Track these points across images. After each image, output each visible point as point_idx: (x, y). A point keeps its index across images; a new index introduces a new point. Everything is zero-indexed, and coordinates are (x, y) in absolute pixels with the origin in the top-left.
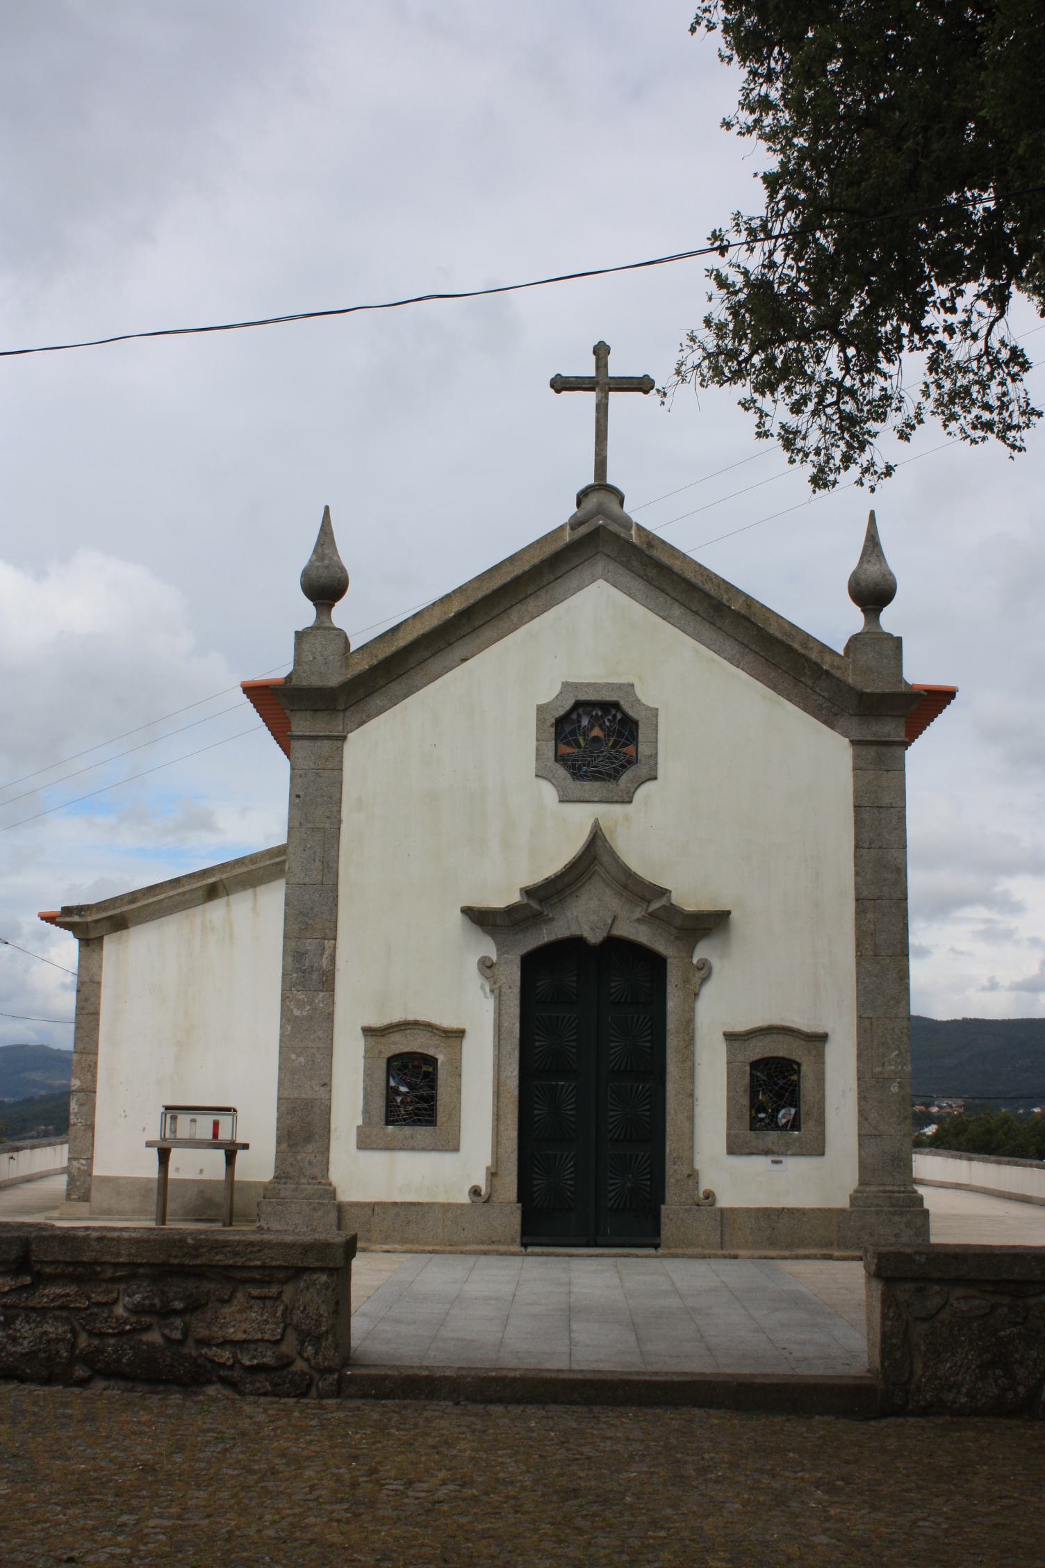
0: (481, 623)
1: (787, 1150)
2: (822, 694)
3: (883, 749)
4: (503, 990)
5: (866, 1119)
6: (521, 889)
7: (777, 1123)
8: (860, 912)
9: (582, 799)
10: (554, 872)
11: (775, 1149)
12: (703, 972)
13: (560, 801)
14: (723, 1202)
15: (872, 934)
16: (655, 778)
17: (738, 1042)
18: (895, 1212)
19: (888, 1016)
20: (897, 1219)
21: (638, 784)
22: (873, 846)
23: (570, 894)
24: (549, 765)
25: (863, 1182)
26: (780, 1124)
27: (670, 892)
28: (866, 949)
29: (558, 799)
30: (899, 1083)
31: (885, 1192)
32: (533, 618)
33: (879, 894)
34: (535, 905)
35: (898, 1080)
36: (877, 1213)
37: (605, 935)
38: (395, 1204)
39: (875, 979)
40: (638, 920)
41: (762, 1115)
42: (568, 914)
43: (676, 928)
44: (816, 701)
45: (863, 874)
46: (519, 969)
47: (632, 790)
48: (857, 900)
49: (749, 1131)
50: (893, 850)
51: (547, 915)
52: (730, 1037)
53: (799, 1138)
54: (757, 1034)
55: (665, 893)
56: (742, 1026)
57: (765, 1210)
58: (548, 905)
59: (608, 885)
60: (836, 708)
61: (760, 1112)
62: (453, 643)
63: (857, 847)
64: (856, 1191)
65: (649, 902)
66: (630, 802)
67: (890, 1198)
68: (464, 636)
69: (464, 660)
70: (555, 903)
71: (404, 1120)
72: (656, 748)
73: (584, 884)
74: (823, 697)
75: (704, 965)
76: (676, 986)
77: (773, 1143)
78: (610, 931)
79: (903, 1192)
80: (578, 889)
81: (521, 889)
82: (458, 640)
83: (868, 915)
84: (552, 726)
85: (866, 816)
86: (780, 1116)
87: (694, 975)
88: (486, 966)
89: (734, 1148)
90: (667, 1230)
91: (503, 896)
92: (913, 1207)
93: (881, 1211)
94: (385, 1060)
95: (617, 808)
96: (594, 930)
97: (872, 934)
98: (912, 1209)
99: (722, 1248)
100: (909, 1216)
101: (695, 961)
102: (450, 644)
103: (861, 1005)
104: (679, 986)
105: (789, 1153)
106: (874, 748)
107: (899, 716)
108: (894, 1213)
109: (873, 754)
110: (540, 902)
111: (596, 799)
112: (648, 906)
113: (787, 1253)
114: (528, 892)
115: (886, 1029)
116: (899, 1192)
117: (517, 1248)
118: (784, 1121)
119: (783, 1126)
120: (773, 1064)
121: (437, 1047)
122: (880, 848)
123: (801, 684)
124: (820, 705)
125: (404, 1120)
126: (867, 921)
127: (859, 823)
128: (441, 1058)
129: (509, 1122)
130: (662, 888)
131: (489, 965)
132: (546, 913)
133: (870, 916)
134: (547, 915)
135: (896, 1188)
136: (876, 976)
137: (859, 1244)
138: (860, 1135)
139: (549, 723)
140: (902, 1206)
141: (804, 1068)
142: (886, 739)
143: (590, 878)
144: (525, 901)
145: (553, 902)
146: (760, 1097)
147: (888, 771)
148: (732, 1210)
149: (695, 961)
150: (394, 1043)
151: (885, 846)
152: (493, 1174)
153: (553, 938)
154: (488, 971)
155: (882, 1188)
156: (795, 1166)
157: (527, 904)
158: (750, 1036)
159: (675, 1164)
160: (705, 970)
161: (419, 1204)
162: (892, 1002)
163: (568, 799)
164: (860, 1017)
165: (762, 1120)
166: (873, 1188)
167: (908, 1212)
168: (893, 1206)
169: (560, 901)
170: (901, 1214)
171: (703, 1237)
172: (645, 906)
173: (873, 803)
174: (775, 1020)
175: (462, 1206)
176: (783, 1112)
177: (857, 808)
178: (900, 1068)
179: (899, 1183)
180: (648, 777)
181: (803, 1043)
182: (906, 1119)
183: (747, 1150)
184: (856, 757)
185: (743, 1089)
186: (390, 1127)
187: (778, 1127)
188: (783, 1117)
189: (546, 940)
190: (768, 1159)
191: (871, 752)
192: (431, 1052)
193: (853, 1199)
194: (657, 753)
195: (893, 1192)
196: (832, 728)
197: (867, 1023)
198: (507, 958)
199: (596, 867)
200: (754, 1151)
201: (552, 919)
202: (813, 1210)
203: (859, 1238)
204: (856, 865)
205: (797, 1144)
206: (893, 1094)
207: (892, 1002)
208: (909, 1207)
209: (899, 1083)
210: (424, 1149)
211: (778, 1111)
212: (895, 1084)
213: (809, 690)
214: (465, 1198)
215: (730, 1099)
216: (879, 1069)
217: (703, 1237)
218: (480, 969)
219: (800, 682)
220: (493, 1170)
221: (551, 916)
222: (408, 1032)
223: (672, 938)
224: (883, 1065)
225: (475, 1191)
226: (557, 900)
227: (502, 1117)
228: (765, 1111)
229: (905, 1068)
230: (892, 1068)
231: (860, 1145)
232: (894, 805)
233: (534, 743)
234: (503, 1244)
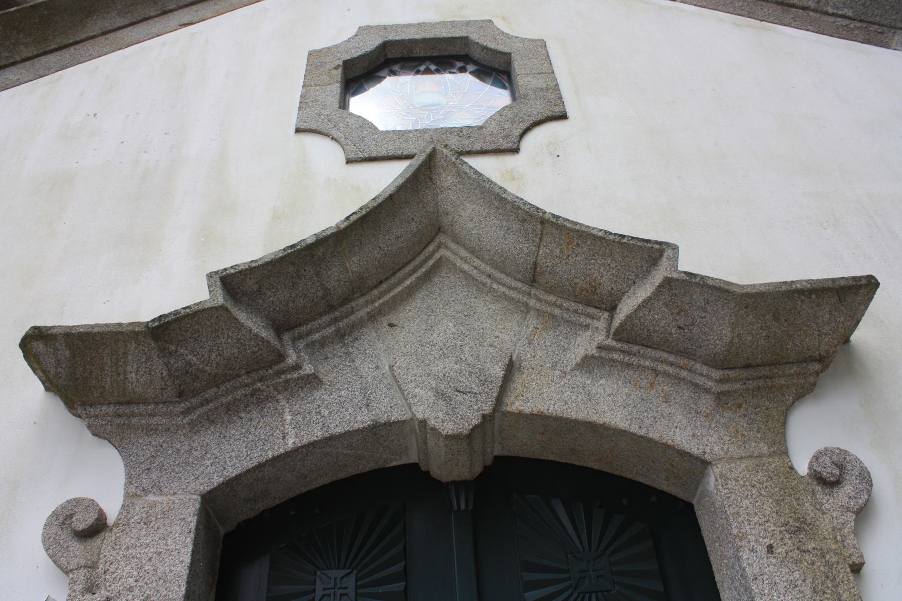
2: (840, 12)
6: (210, 276)
9: (399, 153)
12: (847, 488)
13: (349, 161)
16: (563, 117)
23: (372, 318)
27: (675, 248)
29: (343, 159)
37: (487, 408)
40: (587, 364)
42: (366, 369)
43: (715, 363)
46: (189, 540)
47: (517, 133)
51: (297, 367)
55: (661, 253)
58: (301, 344)
59: (482, 288)
62: (171, 11)
65: (612, 309)
66: (515, 150)
70: (323, 343)
72: (555, 79)
73: (410, 292)
74: (842, 16)
75: (841, 467)
76: (770, 549)
78: (499, 400)
80: (394, 304)
81: (210, 276)
87: (818, 506)
96: (447, 399)
101: (802, 467)
102: (165, 13)
104: (780, 550)
110: (279, 329)
112: (612, 317)
130: (648, 241)
131: (81, 526)
132: (292, 358)
134: (297, 367)
143: (427, 277)
144: (220, 300)
149: (802, 467)
154: (77, 547)
157: (222, 308)
163: (366, 155)
169: (341, 336)
172: (601, 324)
180: (548, 113)
189: (291, 443)
194: (557, 85)
198: (153, 505)
199: (443, 252)
201: (313, 381)
213: (811, 14)
218: (51, 544)
221: (308, 369)
223: (706, 403)
226: (330, 330)
233: (299, 90)
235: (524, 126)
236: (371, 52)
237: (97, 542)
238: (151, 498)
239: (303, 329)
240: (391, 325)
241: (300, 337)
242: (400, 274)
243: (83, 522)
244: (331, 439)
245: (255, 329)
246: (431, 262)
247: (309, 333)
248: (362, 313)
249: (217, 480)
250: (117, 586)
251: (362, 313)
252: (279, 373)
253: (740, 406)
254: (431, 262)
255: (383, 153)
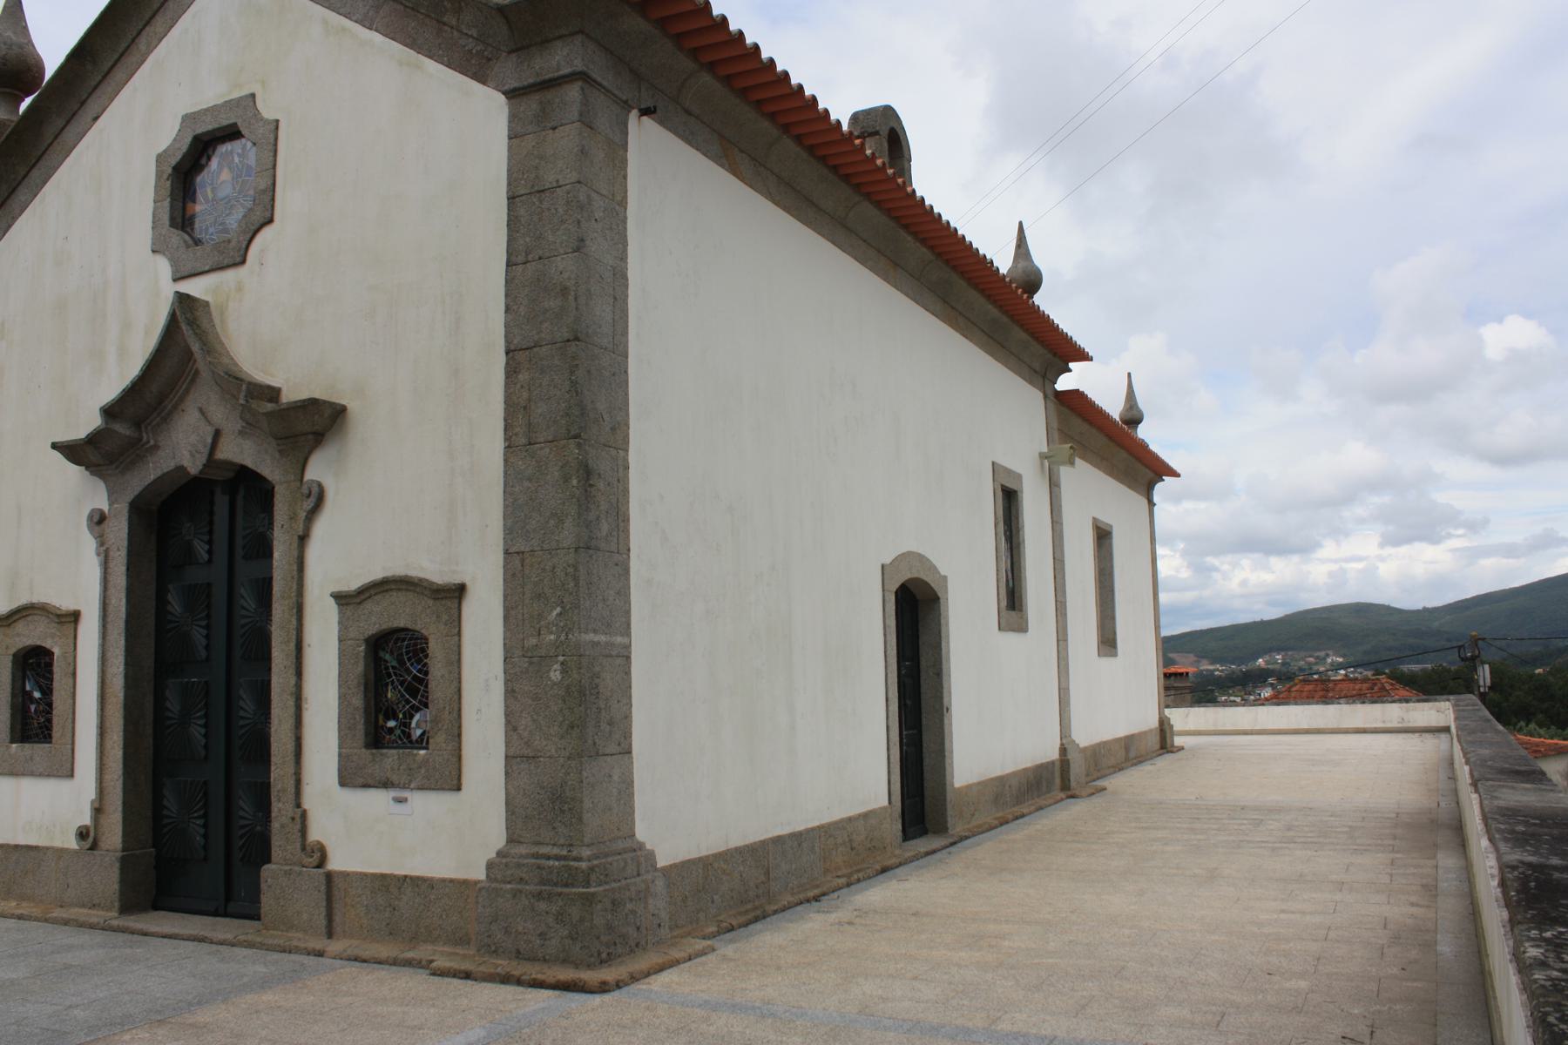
0: (110, 64)
1: (410, 781)
3: (549, 95)
4: (111, 553)
5: (515, 729)
7: (409, 736)
8: (511, 371)
9: (193, 272)
10: (130, 380)
11: (395, 778)
14: (335, 864)
15: (525, 408)
17: (352, 607)
18: (540, 893)
19: (546, 547)
20: (543, 906)
21: (251, 234)
22: (530, 259)
23: (175, 407)
24: (164, 233)
25: (511, 840)
26: (414, 738)
28: (516, 435)
30: (562, 663)
31: (536, 856)
32: (160, 40)
33: (536, 338)
34: (122, 429)
35: (561, 658)
36: (516, 894)
38: (17, 847)
39: (526, 484)
41: (391, 724)
44: (464, 46)
45: (515, 307)
48: (507, 353)
49: (364, 750)
50: (559, 258)
52: (341, 598)
53: (426, 761)
54: (373, 592)
56: (354, 585)
57: (383, 876)
60: (490, 49)
61: (389, 719)
63: (509, 264)
64: (499, 854)
67: (539, 867)
68: (96, 88)
69: (96, 118)
71: (37, 735)
73: (187, 391)
76: (282, 526)
77: (393, 769)
79: (565, 858)
80: (182, 399)
82: (90, 94)
83: (520, 376)
84: (168, 179)
85: (522, 212)
86: (413, 725)
88: (98, 520)
89: (349, 777)
90: (267, 901)
91: (86, 422)
92: (573, 885)
93: (521, 892)
94: (11, 658)
95: (229, 276)
97: (525, 408)
98: (566, 890)
99: (330, 934)
100: (560, 903)
103: (509, 532)
105: (412, 786)
106: (537, 96)
107: (572, 34)
108: (539, 896)
109: (534, 106)
111: (207, 268)
113: (384, 951)
114: (109, 412)
115: (544, 570)
116: (557, 858)
117: (112, 917)
118: (419, 732)
119: (417, 741)
120: (404, 640)
121: (53, 636)
122: (540, 258)
123: (446, 28)
124: (470, 51)
125: (37, 735)
126: (519, 386)
127: (513, 223)
128: (56, 651)
129: (115, 737)
133: (523, 377)
134: (148, 442)
135: (556, 851)
136: (530, 480)
137: (489, 946)
138: (507, 757)
139: (165, 176)
140: (556, 885)
141: (432, 644)
142: (556, 74)
145: (154, 423)
146: (389, 695)
147: (554, 128)
148: (345, 875)
150: (18, 635)
151: (547, 254)
152: (98, 811)
153: (159, 473)
154: (97, 528)
155: (535, 849)
156: (426, 805)
158: (363, 597)
159: (279, 801)
160: (318, 499)
161: (36, 848)
162: (552, 522)
164: (507, 552)
165: (391, 730)
166: (523, 850)
167: (560, 894)
168: (543, 882)
170: (549, 897)
171: (305, 916)
173: (533, 186)
174: (397, 568)
175: (61, 852)
176: (417, 717)
177: (511, 199)
178: (563, 638)
179: (562, 841)
180: (262, 221)
181: (431, 602)
182: (572, 727)
183: (361, 780)
184: (513, 118)
185: (356, 681)
186: (14, 745)
187: (411, 742)
188: (418, 725)
189: (152, 477)
190: (393, 793)
191: (531, 104)
192: (48, 644)
193: (490, 866)
195: (549, 858)
196: (484, 83)
197: (517, 561)
200: (370, 782)
201: (156, 447)
202: (443, 880)
203: (489, 936)
204: (507, 296)
205: (423, 771)
206: (555, 684)
207: (552, 522)
208: (566, 885)
209: (562, 663)
210: (41, 775)
211: (412, 717)
212: (555, 666)
214: (72, 843)
215: (342, 698)
216: (533, 641)
217: (305, 916)
219: (445, 24)
220: (97, 805)
222: (29, 618)
224: (539, 634)
225: (82, 834)
226: (158, 419)
227: (108, 730)
228: (395, 718)
229: (570, 636)
230: (552, 637)
231: (507, 773)
232: (561, 183)
233: (151, 205)
234: (103, 909)
235: (248, 236)
236: (187, 151)
237: (103, 526)
238: (116, 506)
239: (148, 421)
240: (183, 411)
241: (149, 424)
242: (180, 383)
243: (96, 518)
244: (164, 475)
245: (123, 432)
246: (193, 372)
247: (152, 421)
248: (170, 407)
249: (132, 497)
250: (110, 543)
251: (170, 407)
252: (143, 445)
253: (289, 455)
254: (193, 372)
255: (186, 274)
